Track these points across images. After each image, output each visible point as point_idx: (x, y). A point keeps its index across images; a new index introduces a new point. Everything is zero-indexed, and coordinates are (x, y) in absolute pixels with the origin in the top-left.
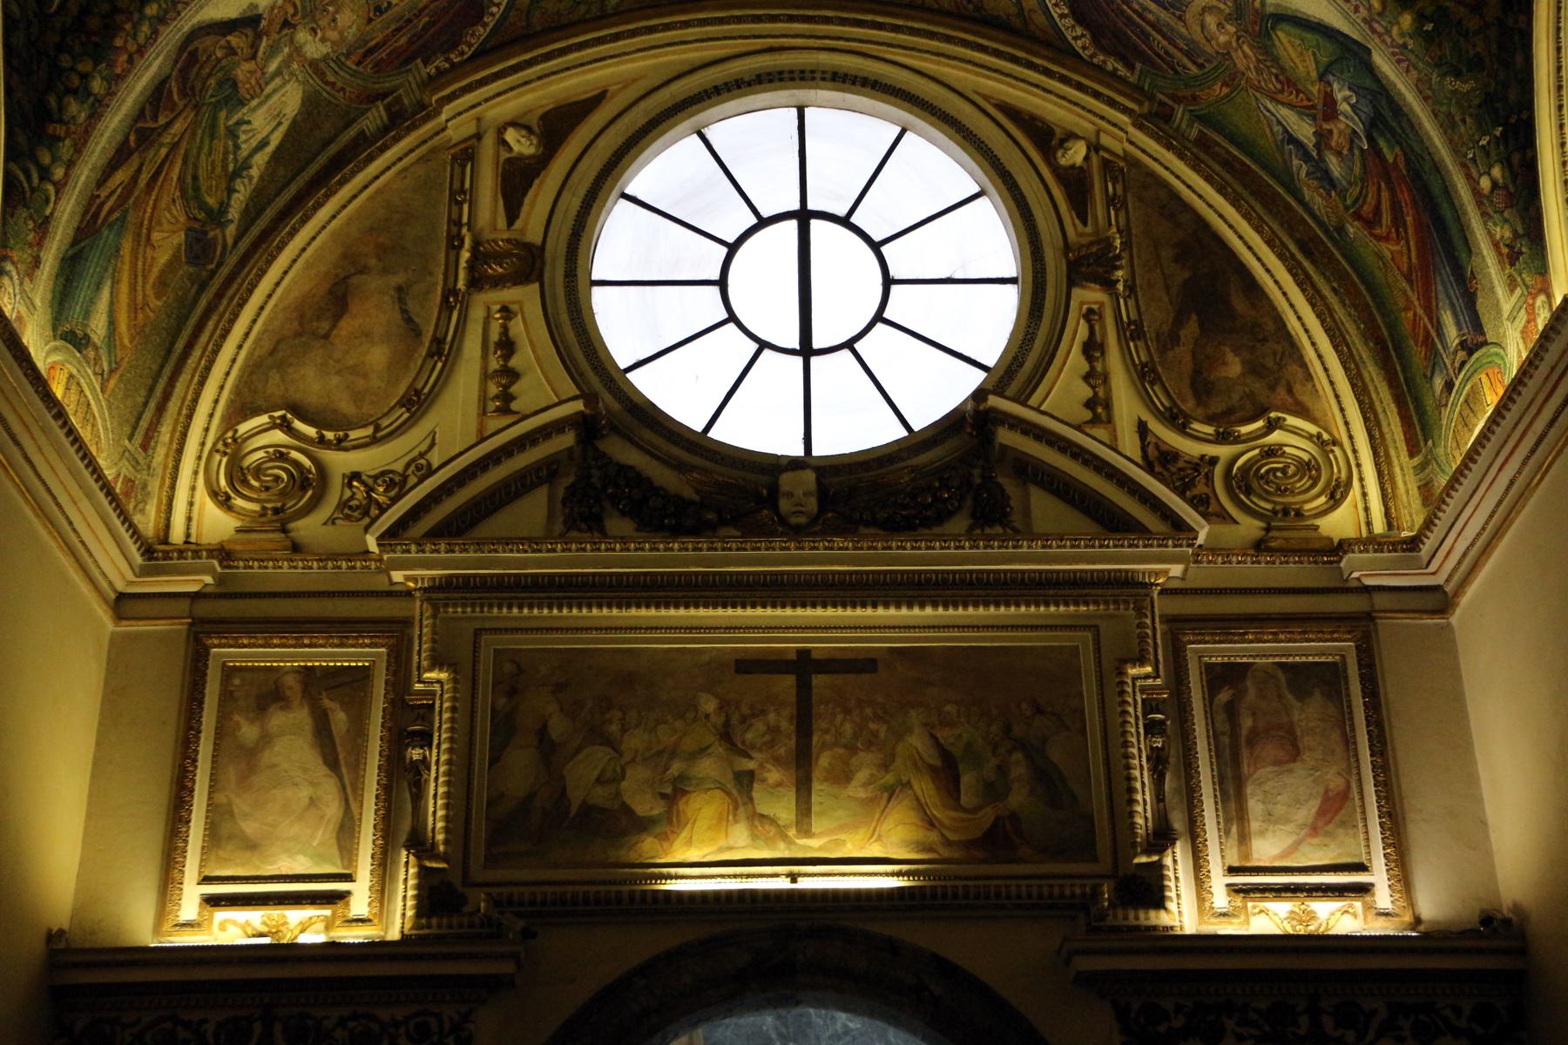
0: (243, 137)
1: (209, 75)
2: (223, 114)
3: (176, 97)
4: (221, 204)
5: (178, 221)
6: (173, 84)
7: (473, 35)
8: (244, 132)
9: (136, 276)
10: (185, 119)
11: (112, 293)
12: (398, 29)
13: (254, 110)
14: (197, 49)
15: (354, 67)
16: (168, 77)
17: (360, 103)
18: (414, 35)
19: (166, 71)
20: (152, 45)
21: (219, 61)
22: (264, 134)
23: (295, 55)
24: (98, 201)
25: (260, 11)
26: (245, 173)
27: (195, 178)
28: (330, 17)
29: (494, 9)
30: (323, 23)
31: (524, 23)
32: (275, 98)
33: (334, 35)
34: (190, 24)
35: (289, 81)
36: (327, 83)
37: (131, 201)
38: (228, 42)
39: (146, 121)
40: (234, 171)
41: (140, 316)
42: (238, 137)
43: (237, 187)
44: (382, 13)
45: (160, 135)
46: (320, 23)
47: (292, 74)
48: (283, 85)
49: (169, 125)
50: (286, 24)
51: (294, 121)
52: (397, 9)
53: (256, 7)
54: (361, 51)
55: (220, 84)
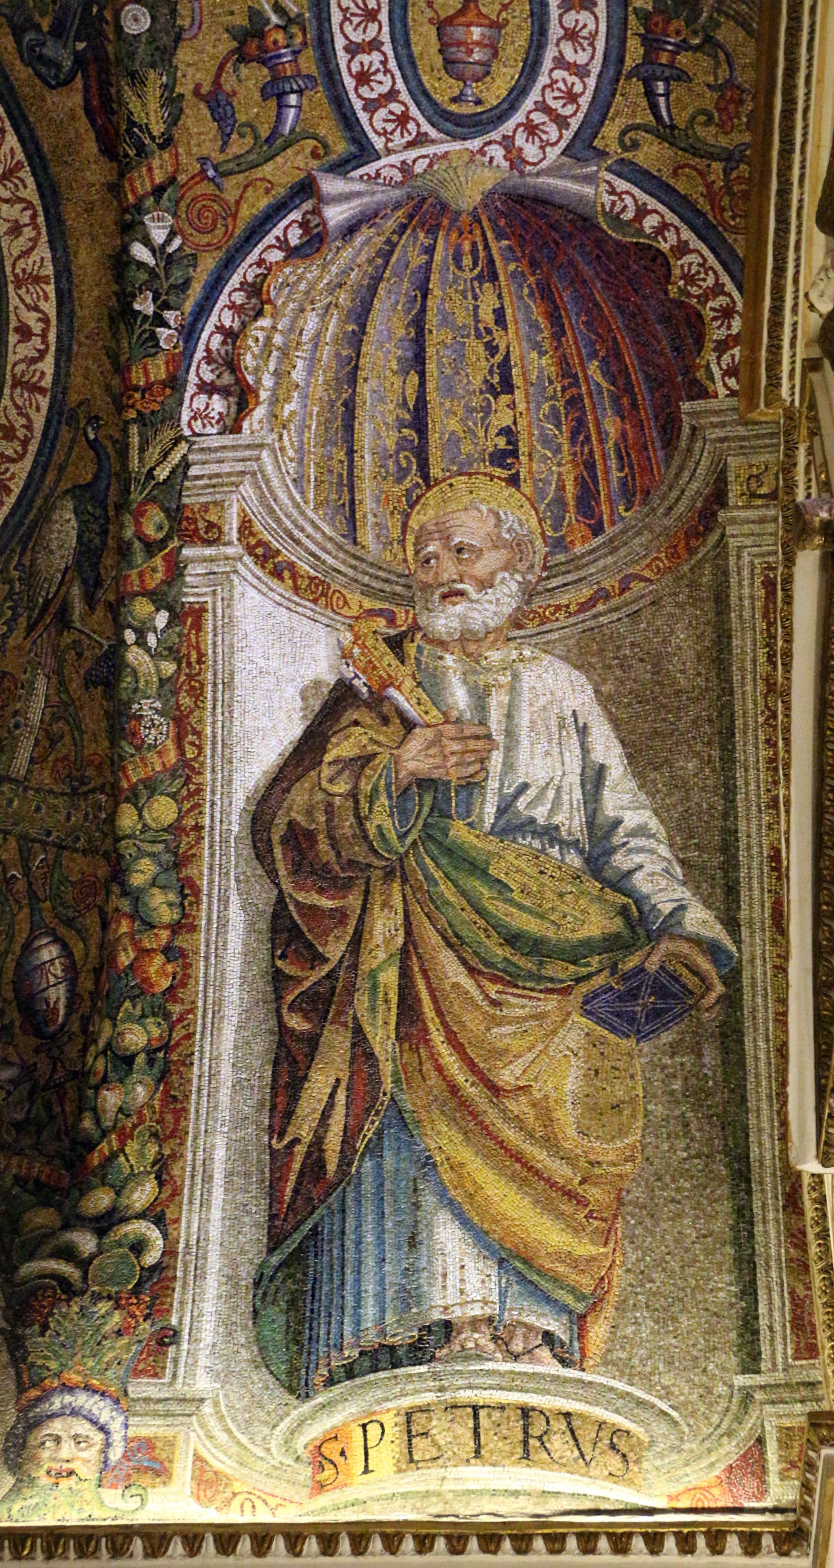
0: (540, 814)
1: (360, 821)
2: (459, 831)
3: (327, 903)
4: (624, 911)
5: (539, 1017)
6: (301, 897)
7: (690, 279)
8: (530, 805)
9: (518, 1157)
10: (386, 905)
11: (465, 1222)
12: (578, 429)
13: (509, 766)
14: (292, 825)
15: (600, 540)
16: (281, 900)
17: (691, 551)
18: (615, 400)
19: (265, 897)
20: (198, 902)
21: (353, 795)
22: (574, 766)
23: (472, 648)
24: (300, 1150)
25: (332, 680)
26: (617, 839)
27: (513, 939)
28: (445, 555)
29: (650, 222)
30: (448, 569)
31: (717, 167)
32: (524, 719)
33: (491, 560)
34: (234, 818)
35: (516, 676)
36: (583, 607)
37: (388, 1085)
38: (335, 762)
39: (299, 981)
40: (587, 861)
41: (593, 1193)
42: (532, 821)
43: (625, 867)
44: (515, 453)
45: (355, 966)
46: (445, 577)
47: (507, 666)
48: (513, 690)
49: (357, 942)
50: (396, 644)
51: (603, 700)
52: (522, 422)
53: (317, 684)
54: (571, 516)
55: (401, 810)
